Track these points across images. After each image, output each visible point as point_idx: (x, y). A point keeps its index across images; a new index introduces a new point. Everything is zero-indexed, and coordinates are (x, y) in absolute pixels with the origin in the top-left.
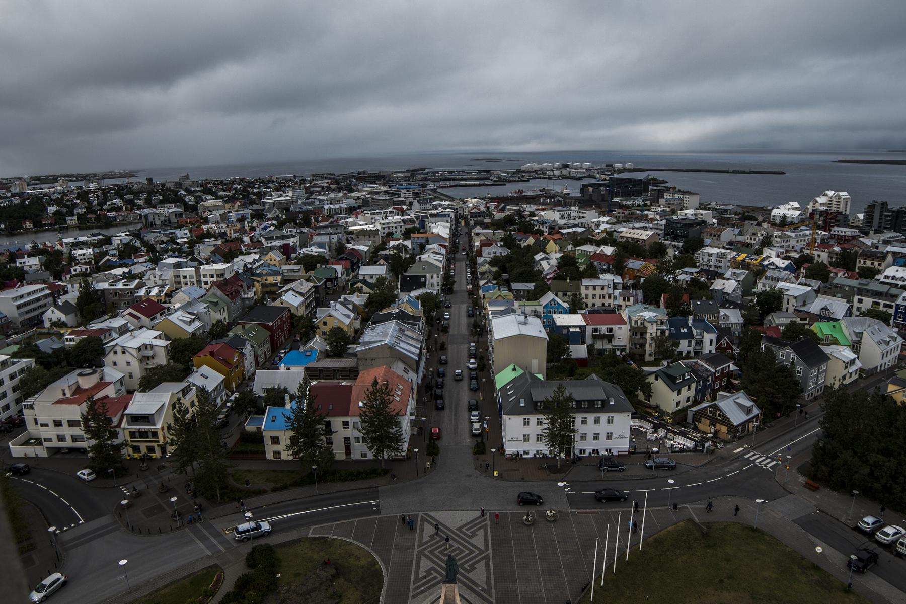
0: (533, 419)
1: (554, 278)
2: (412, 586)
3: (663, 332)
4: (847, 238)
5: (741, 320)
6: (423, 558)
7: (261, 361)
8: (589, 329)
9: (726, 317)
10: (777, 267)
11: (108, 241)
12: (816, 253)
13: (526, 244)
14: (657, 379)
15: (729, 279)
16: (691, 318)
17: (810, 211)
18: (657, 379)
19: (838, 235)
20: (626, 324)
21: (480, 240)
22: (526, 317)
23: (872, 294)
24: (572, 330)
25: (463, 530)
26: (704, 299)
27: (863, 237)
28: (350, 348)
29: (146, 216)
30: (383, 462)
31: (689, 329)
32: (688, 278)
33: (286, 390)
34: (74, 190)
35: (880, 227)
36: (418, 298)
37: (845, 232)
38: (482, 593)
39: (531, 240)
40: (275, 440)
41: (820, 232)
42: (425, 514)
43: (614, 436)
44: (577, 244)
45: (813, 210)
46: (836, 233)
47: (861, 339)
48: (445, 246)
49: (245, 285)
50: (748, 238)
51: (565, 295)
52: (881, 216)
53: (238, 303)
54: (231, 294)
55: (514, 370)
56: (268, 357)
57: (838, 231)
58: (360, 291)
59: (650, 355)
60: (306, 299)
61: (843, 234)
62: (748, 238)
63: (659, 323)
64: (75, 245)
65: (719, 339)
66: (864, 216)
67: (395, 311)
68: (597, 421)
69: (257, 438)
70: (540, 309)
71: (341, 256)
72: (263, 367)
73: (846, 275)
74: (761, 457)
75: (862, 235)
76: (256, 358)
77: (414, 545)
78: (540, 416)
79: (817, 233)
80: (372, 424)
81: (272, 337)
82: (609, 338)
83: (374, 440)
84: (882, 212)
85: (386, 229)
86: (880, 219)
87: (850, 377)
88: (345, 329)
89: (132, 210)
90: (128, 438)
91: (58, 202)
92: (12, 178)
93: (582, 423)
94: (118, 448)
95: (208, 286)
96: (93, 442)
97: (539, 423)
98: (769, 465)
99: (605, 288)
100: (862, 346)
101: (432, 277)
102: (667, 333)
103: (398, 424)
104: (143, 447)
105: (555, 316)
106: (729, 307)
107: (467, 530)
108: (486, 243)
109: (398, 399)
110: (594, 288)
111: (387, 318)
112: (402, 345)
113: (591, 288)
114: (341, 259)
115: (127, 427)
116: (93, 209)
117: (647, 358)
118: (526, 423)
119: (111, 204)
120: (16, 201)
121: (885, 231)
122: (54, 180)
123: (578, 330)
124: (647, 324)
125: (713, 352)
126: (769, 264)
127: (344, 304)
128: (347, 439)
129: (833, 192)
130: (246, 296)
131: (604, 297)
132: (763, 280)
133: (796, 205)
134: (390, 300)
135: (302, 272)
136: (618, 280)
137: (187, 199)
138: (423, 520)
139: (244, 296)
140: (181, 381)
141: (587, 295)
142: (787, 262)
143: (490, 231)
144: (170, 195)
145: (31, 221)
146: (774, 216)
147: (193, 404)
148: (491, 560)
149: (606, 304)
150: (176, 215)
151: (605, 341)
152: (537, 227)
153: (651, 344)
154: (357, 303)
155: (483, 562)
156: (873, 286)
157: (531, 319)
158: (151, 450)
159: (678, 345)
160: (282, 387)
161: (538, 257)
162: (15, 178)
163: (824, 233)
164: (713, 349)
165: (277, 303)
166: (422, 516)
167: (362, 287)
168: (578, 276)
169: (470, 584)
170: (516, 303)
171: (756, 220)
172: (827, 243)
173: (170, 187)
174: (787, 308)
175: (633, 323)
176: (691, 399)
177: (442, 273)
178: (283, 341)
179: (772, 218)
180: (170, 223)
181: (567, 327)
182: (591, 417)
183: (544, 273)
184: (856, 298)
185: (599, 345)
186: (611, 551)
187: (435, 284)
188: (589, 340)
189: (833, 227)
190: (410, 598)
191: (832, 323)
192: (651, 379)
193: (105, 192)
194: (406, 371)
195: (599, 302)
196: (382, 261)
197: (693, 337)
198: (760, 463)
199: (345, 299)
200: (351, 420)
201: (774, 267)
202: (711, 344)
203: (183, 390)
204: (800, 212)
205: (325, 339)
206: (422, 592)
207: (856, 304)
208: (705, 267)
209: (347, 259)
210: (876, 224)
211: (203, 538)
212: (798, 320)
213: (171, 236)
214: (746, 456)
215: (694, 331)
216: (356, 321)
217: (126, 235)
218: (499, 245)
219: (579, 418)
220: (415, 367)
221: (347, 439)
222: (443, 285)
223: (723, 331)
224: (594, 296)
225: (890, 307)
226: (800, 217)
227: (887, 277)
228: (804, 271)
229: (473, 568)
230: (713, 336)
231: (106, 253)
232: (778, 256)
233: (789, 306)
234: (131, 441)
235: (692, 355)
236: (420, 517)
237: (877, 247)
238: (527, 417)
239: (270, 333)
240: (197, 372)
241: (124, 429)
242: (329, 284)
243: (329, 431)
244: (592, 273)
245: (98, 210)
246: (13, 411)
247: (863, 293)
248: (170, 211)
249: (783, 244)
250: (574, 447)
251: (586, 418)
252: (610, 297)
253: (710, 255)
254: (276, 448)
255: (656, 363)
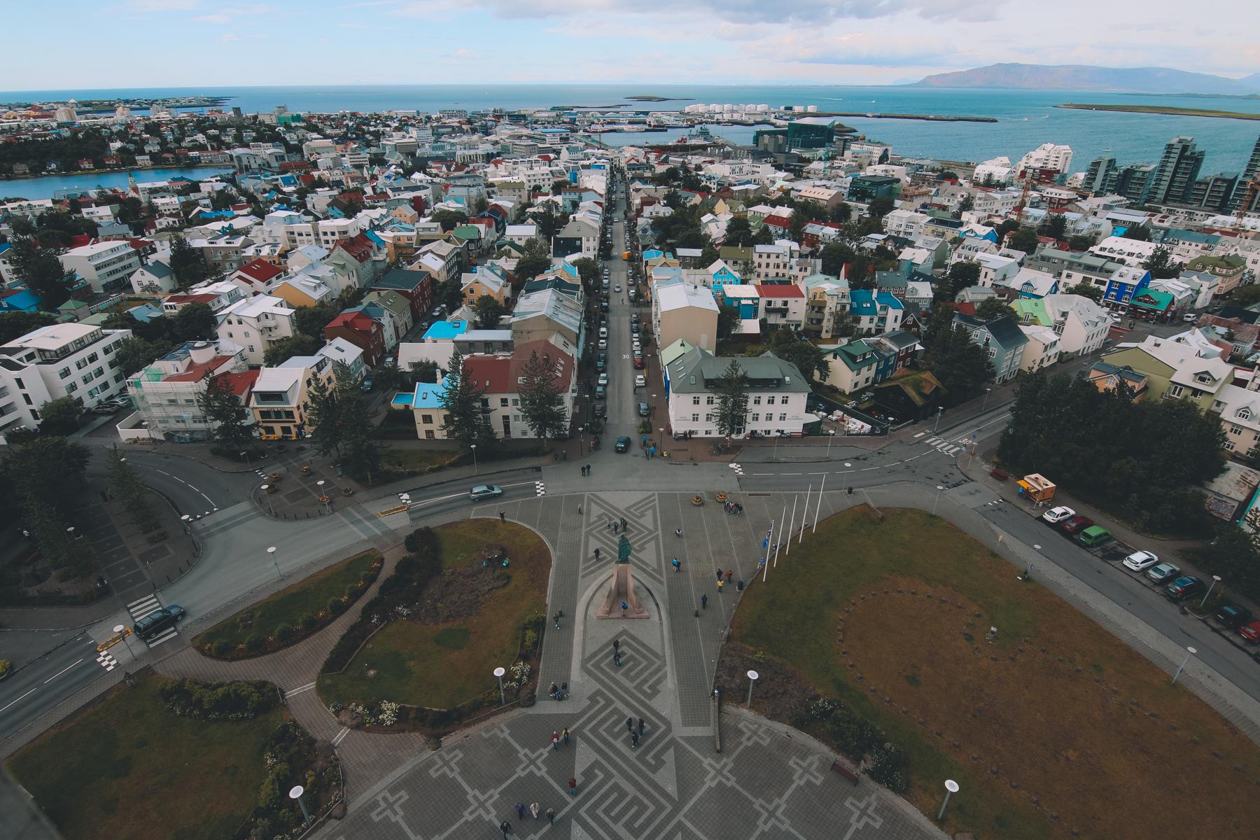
0: (703, 398)
1: (723, 244)
2: (581, 567)
3: (844, 307)
4: (1061, 201)
5: (931, 295)
6: (591, 538)
7: (402, 333)
8: (763, 303)
9: (914, 290)
10: (976, 235)
11: (195, 187)
13: (692, 203)
14: (835, 357)
15: (920, 248)
16: (875, 291)
17: (1022, 168)
18: (835, 357)
19: (1051, 198)
20: (803, 296)
21: (641, 198)
22: (696, 287)
23: (1084, 268)
24: (743, 302)
25: (632, 510)
26: (891, 270)
27: (1080, 201)
28: (502, 319)
29: (239, 157)
30: (545, 441)
31: (873, 303)
32: (873, 245)
33: (435, 365)
34: (140, 120)
36: (574, 264)
37: (1060, 195)
38: (653, 573)
39: (697, 199)
40: (427, 419)
42: (593, 495)
43: (787, 417)
44: (750, 204)
46: (1049, 195)
47: (1066, 319)
48: (600, 204)
49: (374, 245)
51: (735, 263)
53: (368, 265)
54: (360, 255)
55: (682, 345)
56: (409, 328)
57: (1051, 193)
58: (508, 255)
59: (827, 331)
60: (447, 263)
61: (1057, 196)
63: (840, 296)
64: (154, 192)
65: (904, 316)
67: (551, 278)
68: (771, 401)
69: (408, 415)
70: (710, 279)
71: (481, 214)
72: (406, 339)
73: (1056, 246)
74: (943, 442)
75: (1079, 199)
76: (396, 329)
77: (581, 526)
78: (711, 395)
80: (533, 402)
81: (412, 306)
82: (783, 312)
83: (534, 418)
85: (532, 181)
87: (1048, 360)
88: (495, 298)
89: (219, 149)
90: (259, 418)
91: (122, 135)
92: (55, 103)
93: (755, 403)
94: (250, 428)
95: (331, 245)
96: (218, 424)
97: (710, 402)
98: (951, 452)
99: (781, 256)
100: (1065, 327)
101: (588, 240)
102: (848, 308)
103: (561, 402)
104: (277, 428)
105: (726, 287)
106: (917, 280)
107: (636, 510)
108: (648, 201)
109: (560, 375)
110: (769, 256)
111: (542, 286)
112: (561, 316)
113: (765, 256)
114: (483, 217)
115: (256, 406)
116: (169, 146)
117: (824, 335)
118: (696, 402)
119: (192, 141)
120: (66, 133)
121: (1108, 194)
122: (110, 108)
123: (750, 302)
124: (826, 298)
125: (897, 329)
126: (967, 231)
127: (491, 269)
128: (506, 418)
129: (1053, 145)
130: (377, 258)
131: (778, 267)
132: (960, 250)
133: (1006, 160)
134: (546, 265)
135: (440, 232)
136: (795, 246)
137: (287, 137)
138: (590, 500)
139: (374, 258)
140: (313, 355)
141: (760, 266)
142: (989, 229)
143: (651, 186)
144: (265, 131)
145: (91, 160)
146: (978, 174)
147: (329, 380)
148: (661, 541)
149: (780, 274)
150: (276, 157)
151: (779, 315)
152: (704, 184)
153: (829, 320)
154: (506, 268)
155: (653, 543)
156: (1087, 259)
157: (701, 289)
158: (286, 430)
159: (858, 321)
160: (431, 362)
161: (705, 219)
162: (58, 103)
164: (897, 326)
165: (415, 267)
166: (588, 497)
167: (510, 251)
168: (751, 242)
169: (640, 564)
170: (685, 271)
173: (264, 122)
174: (984, 282)
175: (811, 296)
176: (870, 380)
177: (599, 236)
178: (425, 310)
179: (975, 176)
180: (270, 167)
181: (739, 299)
182: (765, 397)
183: (713, 237)
184: (1065, 272)
185: (773, 319)
186: (786, 532)
187: (592, 249)
188: (761, 314)
190: (580, 578)
191: (1034, 300)
192: (829, 358)
193: (181, 124)
194: (566, 345)
195: (772, 272)
196: (530, 221)
197: (876, 313)
198: (941, 448)
199: (492, 263)
200: (511, 397)
201: (972, 235)
202: (896, 320)
203: (317, 365)
204: (1009, 169)
205: (474, 310)
206: (592, 572)
207: (1063, 279)
208: (893, 234)
209: (489, 217)
210: (1097, 185)
211: (356, 522)
212: (996, 296)
213: (274, 183)
214: (927, 442)
215: (878, 306)
216: (505, 289)
217: (217, 181)
218: (662, 204)
219: (752, 397)
220: (575, 341)
221: (506, 418)
222: (600, 250)
223: (910, 307)
224: (768, 265)
225: (1103, 283)
227: (1102, 249)
228: (1007, 241)
229: (642, 548)
230: (900, 313)
231: (195, 204)
232: (979, 222)
233: (986, 280)
234: (263, 422)
235: (873, 331)
236: (586, 498)
238: (697, 395)
239: (409, 301)
240: (331, 344)
241: (253, 408)
242: (472, 247)
243: (486, 410)
244: (767, 238)
245: (176, 148)
246: (114, 388)
247: (1074, 267)
248: (269, 152)
250: (744, 429)
251: (759, 397)
252: (785, 266)
253: (900, 218)
254: (429, 427)
255: (834, 339)
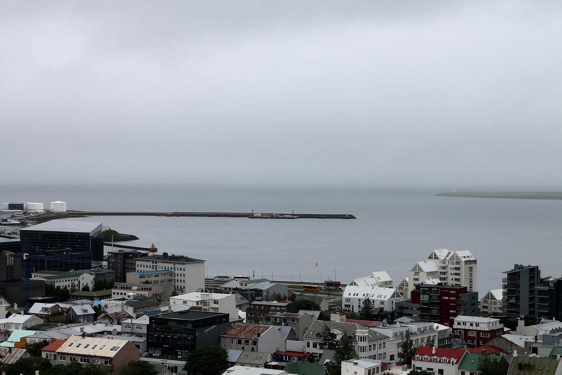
12: (436, 367)
17: (411, 288)
19: (466, 331)
27: (508, 332)
35: (532, 313)
37: (477, 325)
41: (435, 325)
45: (418, 287)
50: (308, 345)
52: (532, 292)
57: (465, 324)
61: (474, 328)
62: (308, 345)
66: (504, 294)
75: (506, 329)
79: (431, 327)
84: (532, 285)
86: (531, 299)
121: (543, 320)
163: (442, 327)
171: (317, 308)
172: (450, 346)
179: (344, 303)
189: (455, 315)
204: (392, 291)
226: (395, 300)
237: (535, 350)
249: (373, 353)
